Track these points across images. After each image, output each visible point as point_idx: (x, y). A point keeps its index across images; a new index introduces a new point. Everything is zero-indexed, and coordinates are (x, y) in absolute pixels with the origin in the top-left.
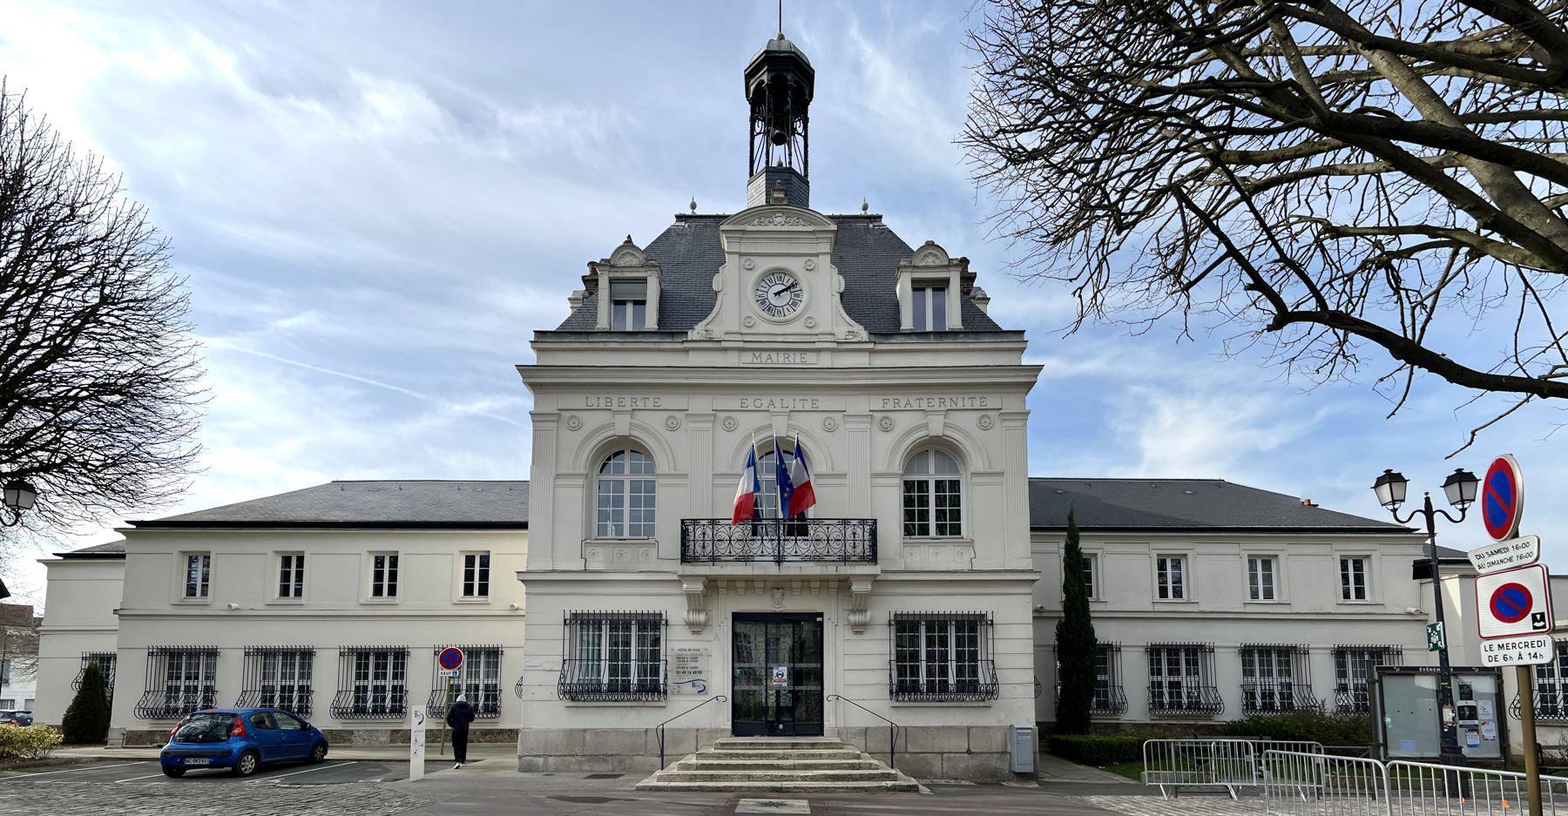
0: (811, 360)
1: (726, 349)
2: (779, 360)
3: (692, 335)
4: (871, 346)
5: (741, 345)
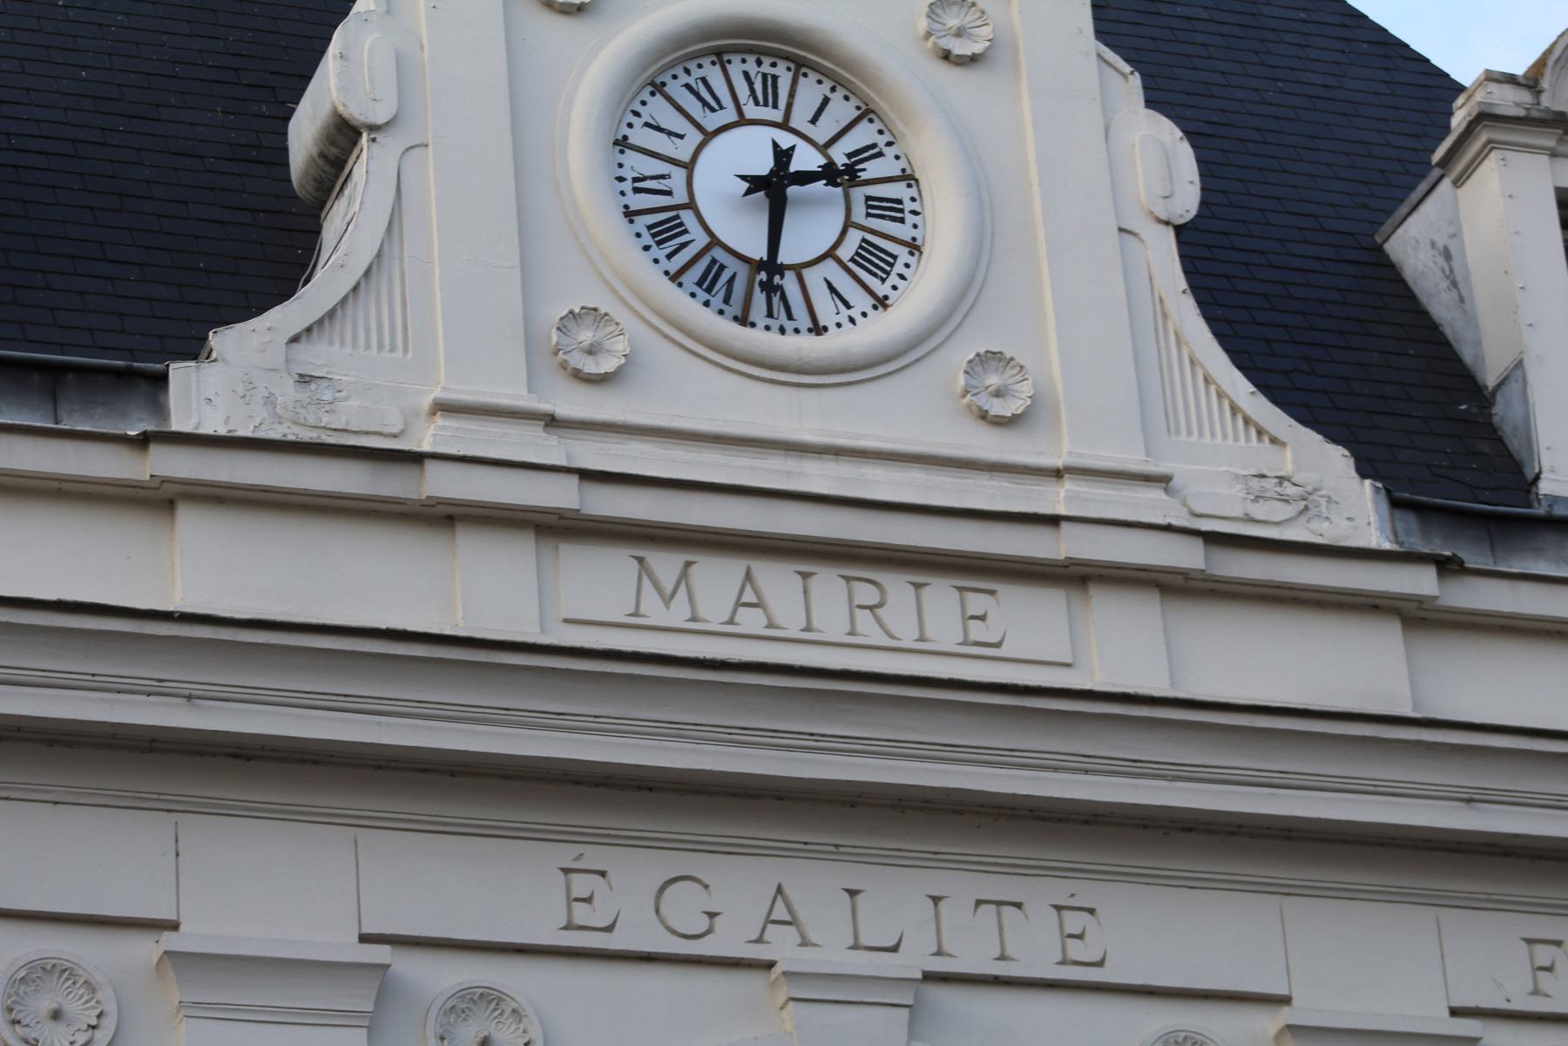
0: (1033, 636)
1: (446, 517)
2: (816, 619)
3: (201, 395)
4: (1420, 582)
5: (561, 495)
